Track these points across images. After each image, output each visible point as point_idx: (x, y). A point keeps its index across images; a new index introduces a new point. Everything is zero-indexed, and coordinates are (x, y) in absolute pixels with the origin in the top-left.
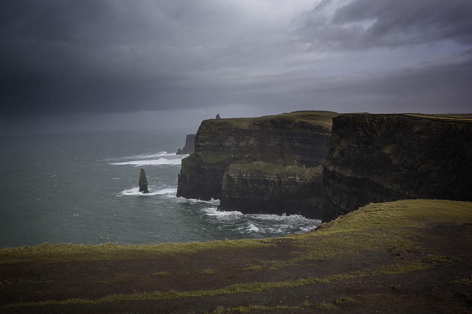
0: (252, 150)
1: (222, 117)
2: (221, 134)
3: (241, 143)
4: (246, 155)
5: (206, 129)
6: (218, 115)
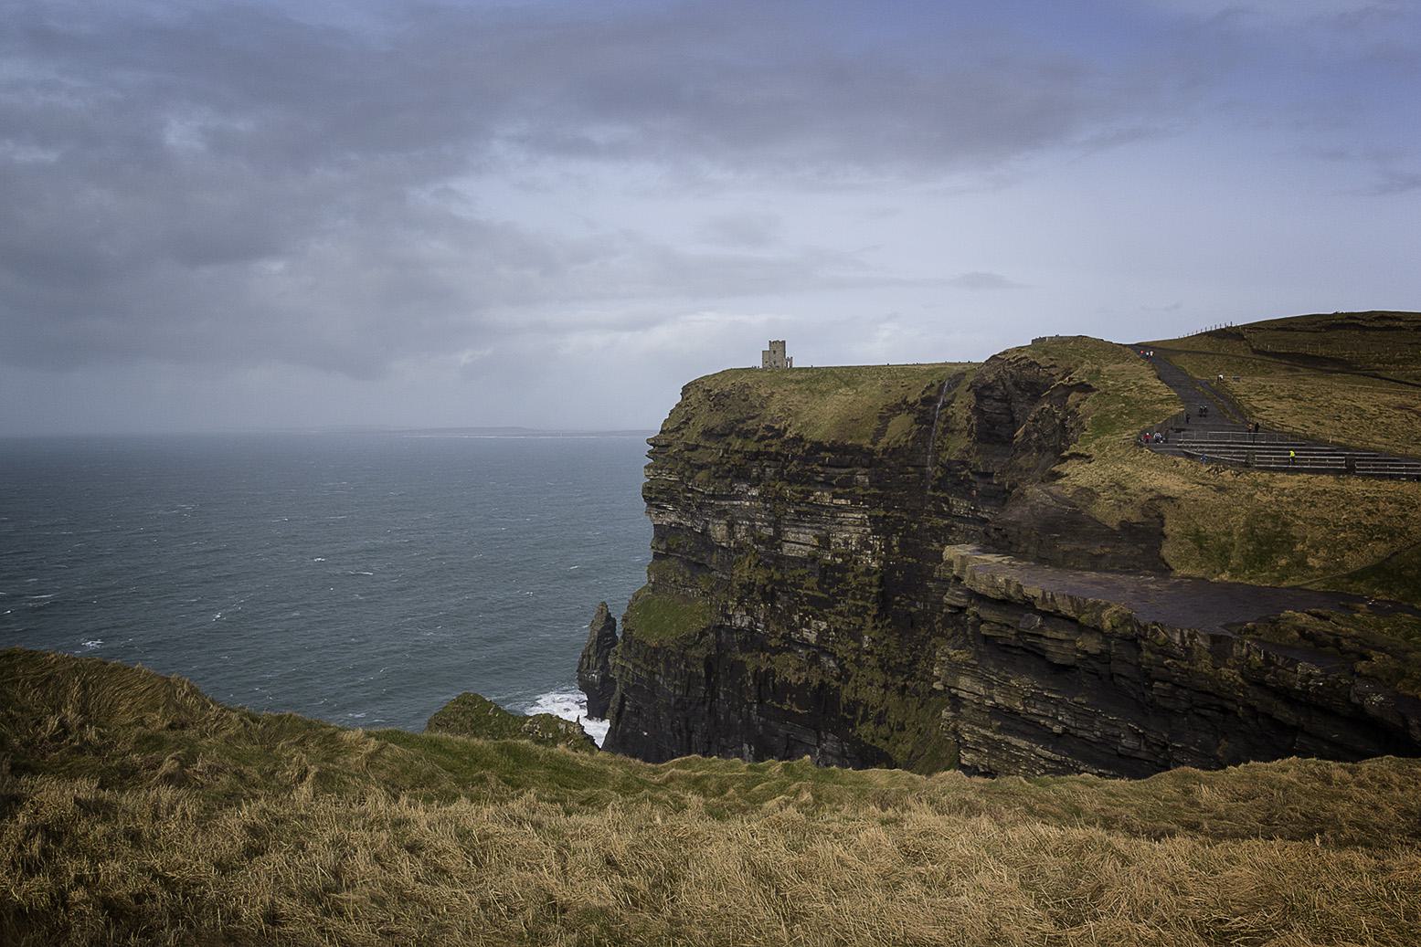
0: (844, 593)
1: (801, 357)
2: (701, 467)
3: (791, 536)
4: (808, 625)
5: (678, 429)
6: (778, 347)
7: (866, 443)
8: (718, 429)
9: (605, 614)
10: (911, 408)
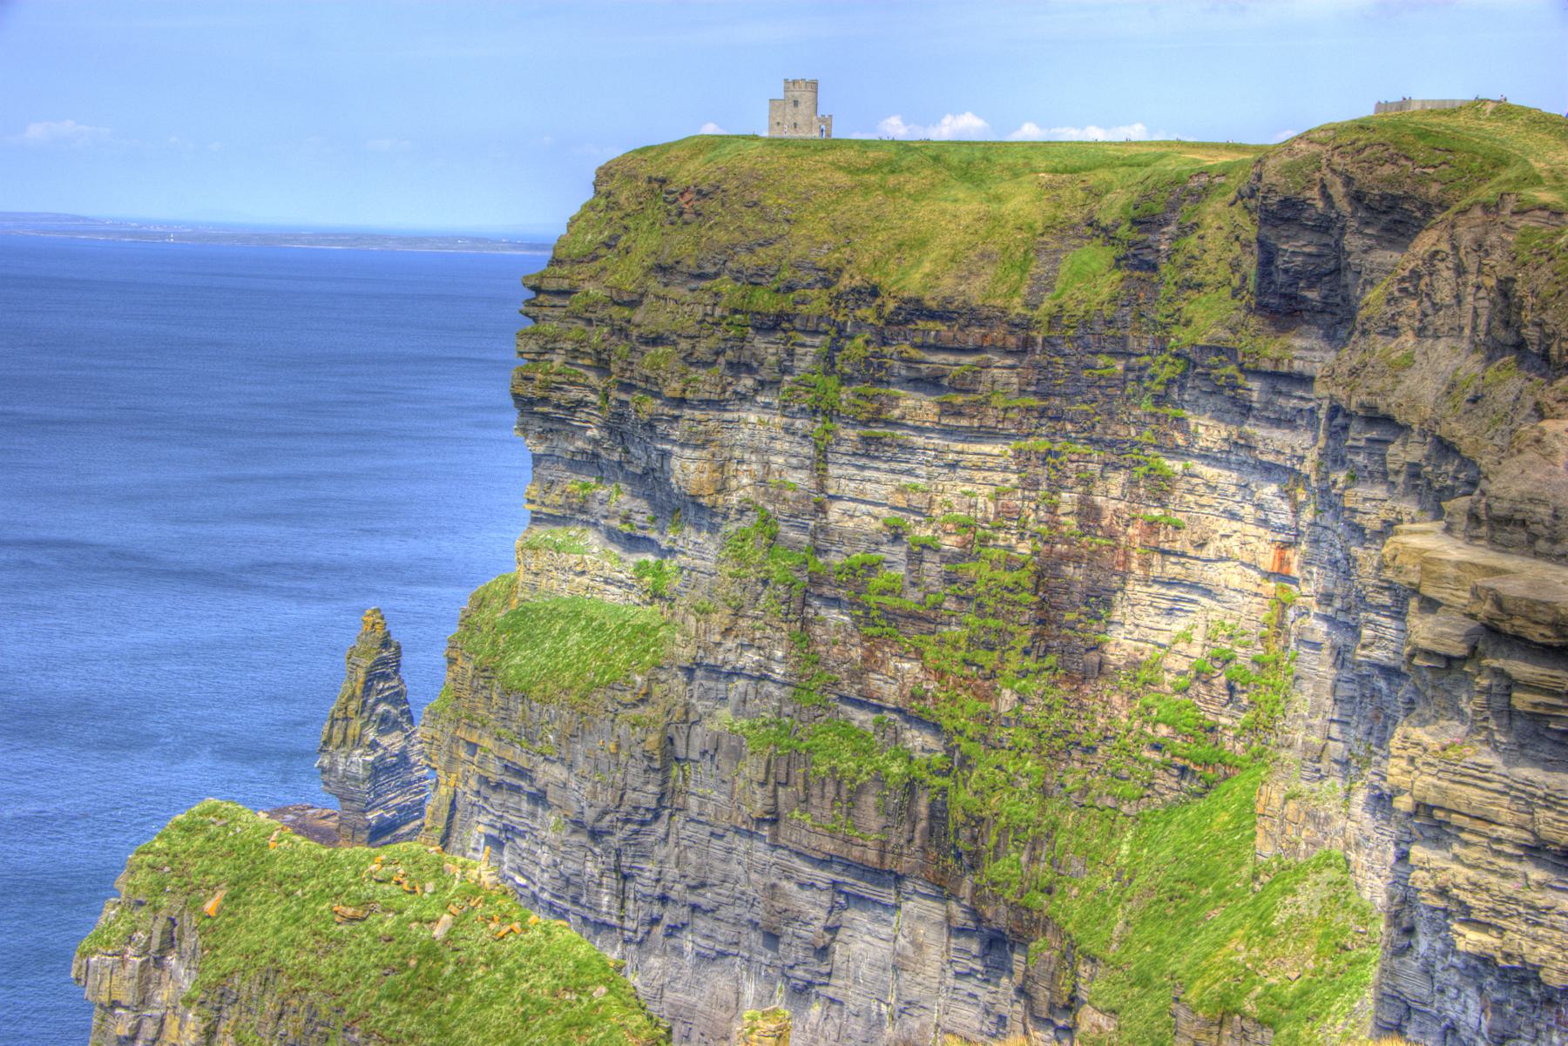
7: (1017, 307)
8: (691, 262)
9: (379, 634)
10: (1107, 234)
